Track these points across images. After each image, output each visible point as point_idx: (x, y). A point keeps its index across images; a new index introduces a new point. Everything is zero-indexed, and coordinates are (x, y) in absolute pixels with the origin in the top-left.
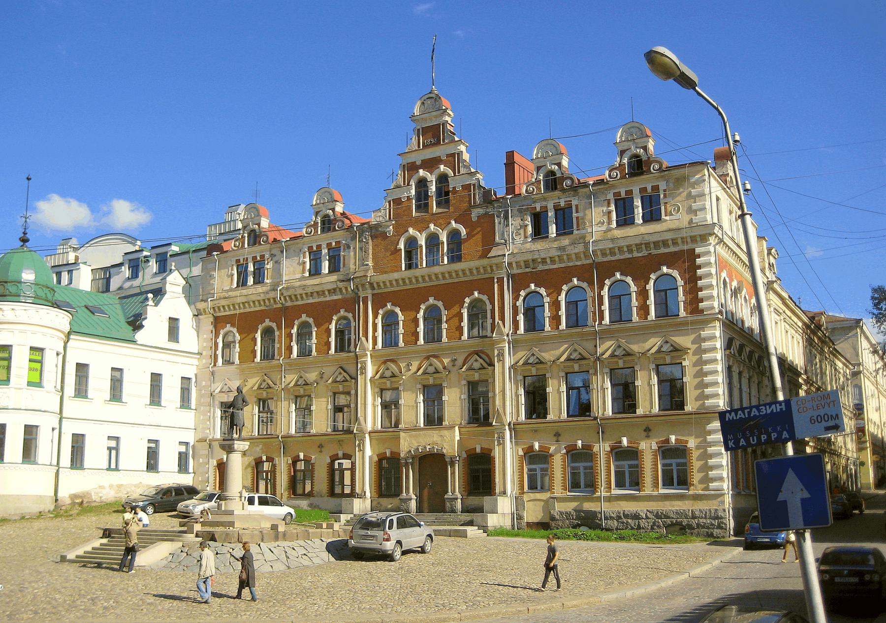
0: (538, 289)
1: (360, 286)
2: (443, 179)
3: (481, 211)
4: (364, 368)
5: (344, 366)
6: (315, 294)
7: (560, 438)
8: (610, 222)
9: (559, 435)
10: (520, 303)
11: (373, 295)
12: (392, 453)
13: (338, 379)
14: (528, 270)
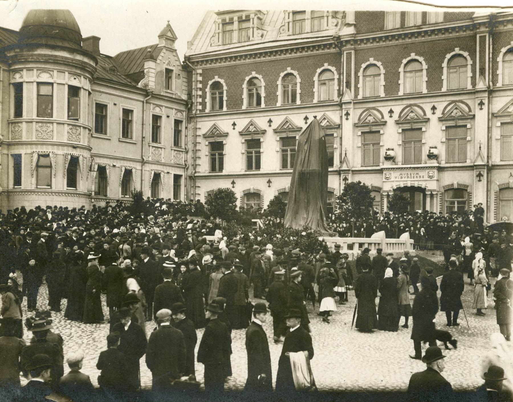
4: (347, 114)
11: (356, 51)
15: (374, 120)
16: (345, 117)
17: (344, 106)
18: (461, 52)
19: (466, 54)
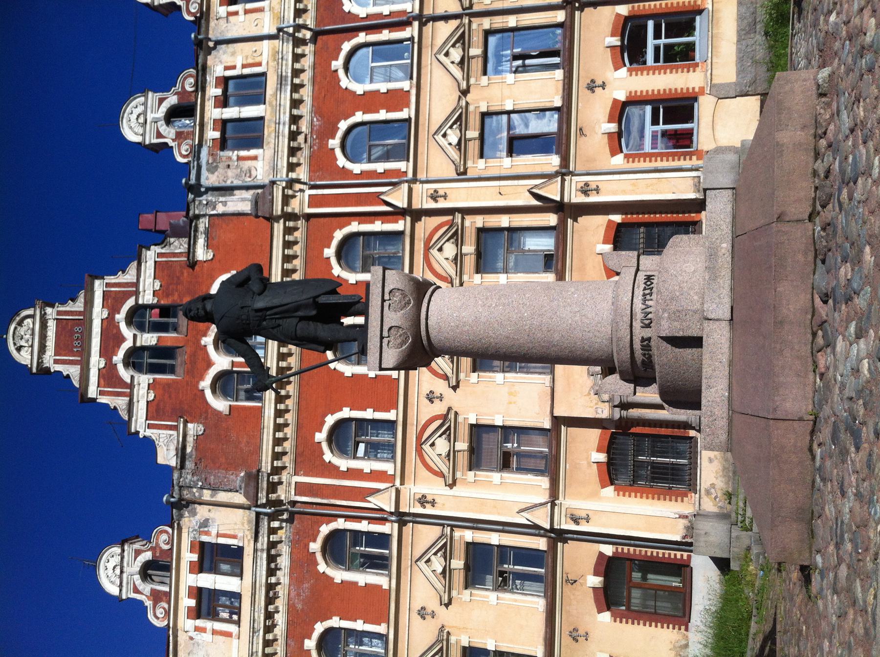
0: (339, 134)
1: (273, 496)
2: (137, 317)
3: (201, 242)
4: (423, 501)
5: (417, 554)
6: (271, 608)
7: (599, 82)
8: (261, 10)
9: (593, 81)
10: (356, 168)
12: (599, 450)
13: (440, 569)
15: (444, 436)
16: (427, 505)
17: (403, 509)
18: (335, 243)
19: (339, 235)
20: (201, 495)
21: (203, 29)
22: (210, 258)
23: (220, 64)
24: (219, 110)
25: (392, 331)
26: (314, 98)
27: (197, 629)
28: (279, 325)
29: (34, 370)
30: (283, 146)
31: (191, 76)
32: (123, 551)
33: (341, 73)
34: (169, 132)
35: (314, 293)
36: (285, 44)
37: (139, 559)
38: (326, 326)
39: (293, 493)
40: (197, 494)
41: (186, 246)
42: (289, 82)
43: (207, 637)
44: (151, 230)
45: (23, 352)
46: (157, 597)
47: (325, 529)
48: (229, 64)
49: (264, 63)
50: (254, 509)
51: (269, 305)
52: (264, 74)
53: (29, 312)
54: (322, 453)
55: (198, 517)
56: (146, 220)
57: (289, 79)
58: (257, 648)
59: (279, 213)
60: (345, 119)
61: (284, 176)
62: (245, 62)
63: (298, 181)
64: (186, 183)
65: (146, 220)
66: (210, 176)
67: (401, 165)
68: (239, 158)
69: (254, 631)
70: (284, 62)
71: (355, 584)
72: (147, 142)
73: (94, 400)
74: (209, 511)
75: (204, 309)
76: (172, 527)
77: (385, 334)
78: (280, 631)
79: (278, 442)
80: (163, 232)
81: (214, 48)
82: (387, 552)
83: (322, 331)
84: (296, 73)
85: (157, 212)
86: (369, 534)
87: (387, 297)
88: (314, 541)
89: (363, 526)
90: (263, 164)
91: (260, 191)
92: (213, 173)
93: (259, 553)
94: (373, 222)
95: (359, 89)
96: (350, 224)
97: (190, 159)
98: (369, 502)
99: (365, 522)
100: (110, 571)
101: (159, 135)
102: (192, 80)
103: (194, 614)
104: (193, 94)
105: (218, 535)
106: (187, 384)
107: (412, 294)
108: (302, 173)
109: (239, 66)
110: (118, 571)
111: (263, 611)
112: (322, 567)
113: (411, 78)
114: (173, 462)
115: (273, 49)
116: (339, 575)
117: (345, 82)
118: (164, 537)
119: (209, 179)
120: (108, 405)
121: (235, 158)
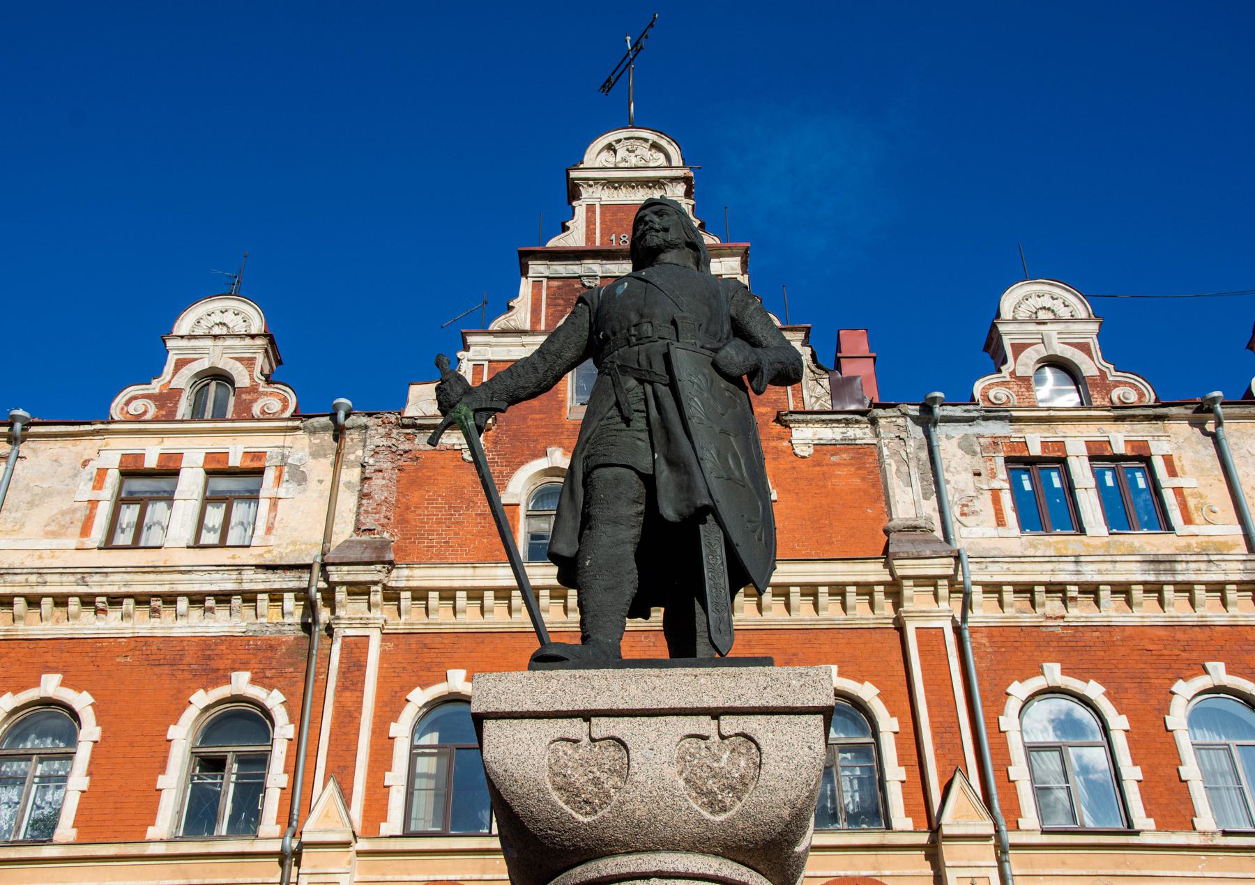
11: (386, 636)
14: (1028, 618)
19: (867, 692)
20: (351, 465)
21: (1237, 410)
22: (797, 451)
23: (1176, 443)
24: (1084, 451)
25: (612, 752)
26: (1141, 629)
27: (102, 472)
28: (627, 421)
29: (573, 174)
30: (1033, 572)
31: (1141, 395)
32: (253, 337)
33: (1202, 682)
34: (1026, 365)
35: (723, 508)
36: (1241, 567)
37: (238, 364)
38: (631, 549)
39: (350, 632)
40: (352, 457)
41: (816, 408)
42: (1163, 578)
43: (85, 491)
44: (838, 350)
45: (605, 154)
46: (167, 400)
47: (274, 700)
48: (1177, 463)
49: (1192, 529)
50: (319, 560)
51: (693, 424)
52: (1169, 528)
53: (677, 159)
54: (424, 686)
55: (311, 462)
56: (855, 342)
57: (1169, 578)
58: (53, 584)
59: (899, 572)
60: (1107, 694)
61: (974, 578)
62: (1186, 492)
63: (967, 605)
64: (934, 399)
65: (855, 342)
66: (955, 442)
67: (1029, 818)
68: (995, 493)
69: (84, 574)
70: (1203, 566)
71: (163, 769)
72: (1002, 328)
73: (524, 272)
74: (321, 481)
75: (670, 246)
76: (294, 416)
77: (602, 727)
78: (88, 624)
79: (448, 595)
80: (838, 367)
81: (1205, 433)
82: (224, 832)
83: (618, 538)
84: (1186, 588)
85: (875, 358)
86: (261, 788)
87: (730, 725)
88: (253, 681)
89: (276, 777)
90: (989, 534)
91: (938, 534)
92: (960, 446)
93: (234, 575)
94: (901, 762)
95: (1177, 718)
96: (892, 714)
97: (981, 404)
98: (324, 787)
99: (284, 780)
100: (217, 318)
101: (1019, 349)
102: (1133, 398)
103: (131, 466)
104: (1106, 403)
105: (275, 501)
106: (557, 427)
107: (744, 815)
108: (984, 612)
109: (1176, 482)
110: (217, 331)
111: (123, 590)
112: (201, 699)
113: (1225, 833)
114: (410, 411)
115: (1225, 543)
116: (182, 736)
117: (1184, 690)
118: (276, 405)
119: (949, 439)
120: (517, 296)
121: (996, 484)
